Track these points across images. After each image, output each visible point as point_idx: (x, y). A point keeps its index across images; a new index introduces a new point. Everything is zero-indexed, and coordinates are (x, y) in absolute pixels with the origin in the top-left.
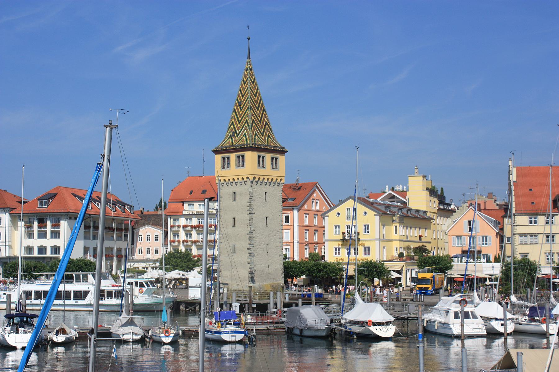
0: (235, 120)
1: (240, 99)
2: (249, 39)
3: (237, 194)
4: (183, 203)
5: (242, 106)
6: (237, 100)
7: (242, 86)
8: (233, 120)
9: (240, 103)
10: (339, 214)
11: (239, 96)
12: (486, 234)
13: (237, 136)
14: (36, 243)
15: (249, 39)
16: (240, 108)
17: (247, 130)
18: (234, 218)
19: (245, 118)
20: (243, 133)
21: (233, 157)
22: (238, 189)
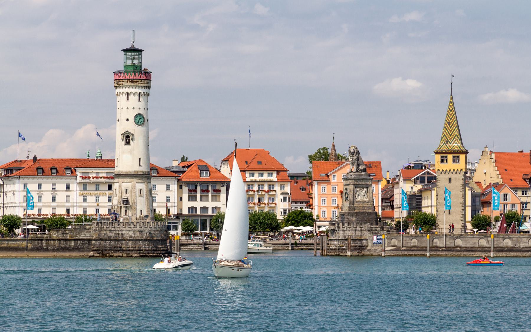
8: (445, 133)
9: (449, 123)
14: (198, 204)
22: (453, 176)
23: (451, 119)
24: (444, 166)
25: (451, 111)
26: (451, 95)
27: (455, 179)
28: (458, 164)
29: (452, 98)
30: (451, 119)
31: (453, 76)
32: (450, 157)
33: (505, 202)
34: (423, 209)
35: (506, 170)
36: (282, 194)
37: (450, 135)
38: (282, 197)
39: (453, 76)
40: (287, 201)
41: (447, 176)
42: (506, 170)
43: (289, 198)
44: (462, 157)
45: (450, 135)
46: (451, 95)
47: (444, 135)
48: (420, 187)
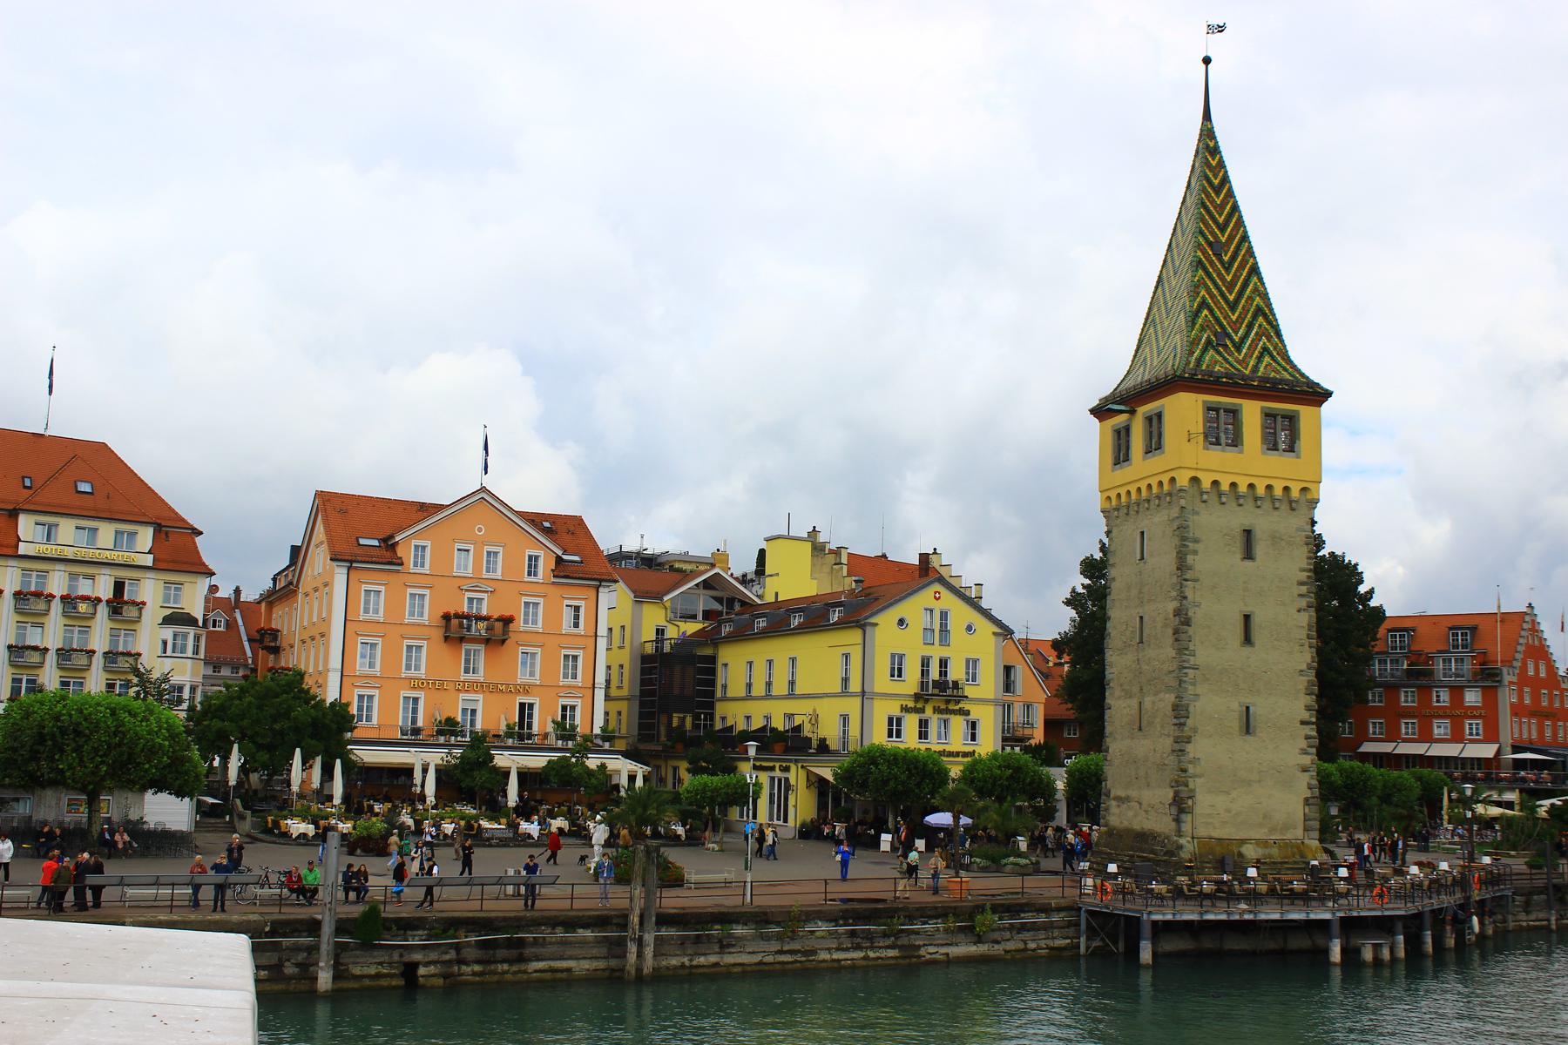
0: (1212, 296)
1: (1215, 236)
2: (1207, 61)
3: (1258, 534)
4: (13, 514)
5: (1226, 259)
6: (1201, 232)
7: (1208, 195)
9: (1217, 248)
10: (901, 622)
13: (1238, 348)
15: (1207, 61)
17: (1269, 338)
18: (1247, 618)
19: (1250, 299)
21: (1252, 412)
22: (1263, 523)
24: (1219, 465)
25: (1218, 193)
26: (1207, 115)
27: (1275, 539)
28: (1288, 459)
29: (1207, 133)
34: (721, 709)
36: (168, 621)
38: (168, 633)
40: (190, 653)
41: (1239, 518)
43: (197, 638)
45: (1233, 307)
46: (1207, 115)
47: (1203, 304)
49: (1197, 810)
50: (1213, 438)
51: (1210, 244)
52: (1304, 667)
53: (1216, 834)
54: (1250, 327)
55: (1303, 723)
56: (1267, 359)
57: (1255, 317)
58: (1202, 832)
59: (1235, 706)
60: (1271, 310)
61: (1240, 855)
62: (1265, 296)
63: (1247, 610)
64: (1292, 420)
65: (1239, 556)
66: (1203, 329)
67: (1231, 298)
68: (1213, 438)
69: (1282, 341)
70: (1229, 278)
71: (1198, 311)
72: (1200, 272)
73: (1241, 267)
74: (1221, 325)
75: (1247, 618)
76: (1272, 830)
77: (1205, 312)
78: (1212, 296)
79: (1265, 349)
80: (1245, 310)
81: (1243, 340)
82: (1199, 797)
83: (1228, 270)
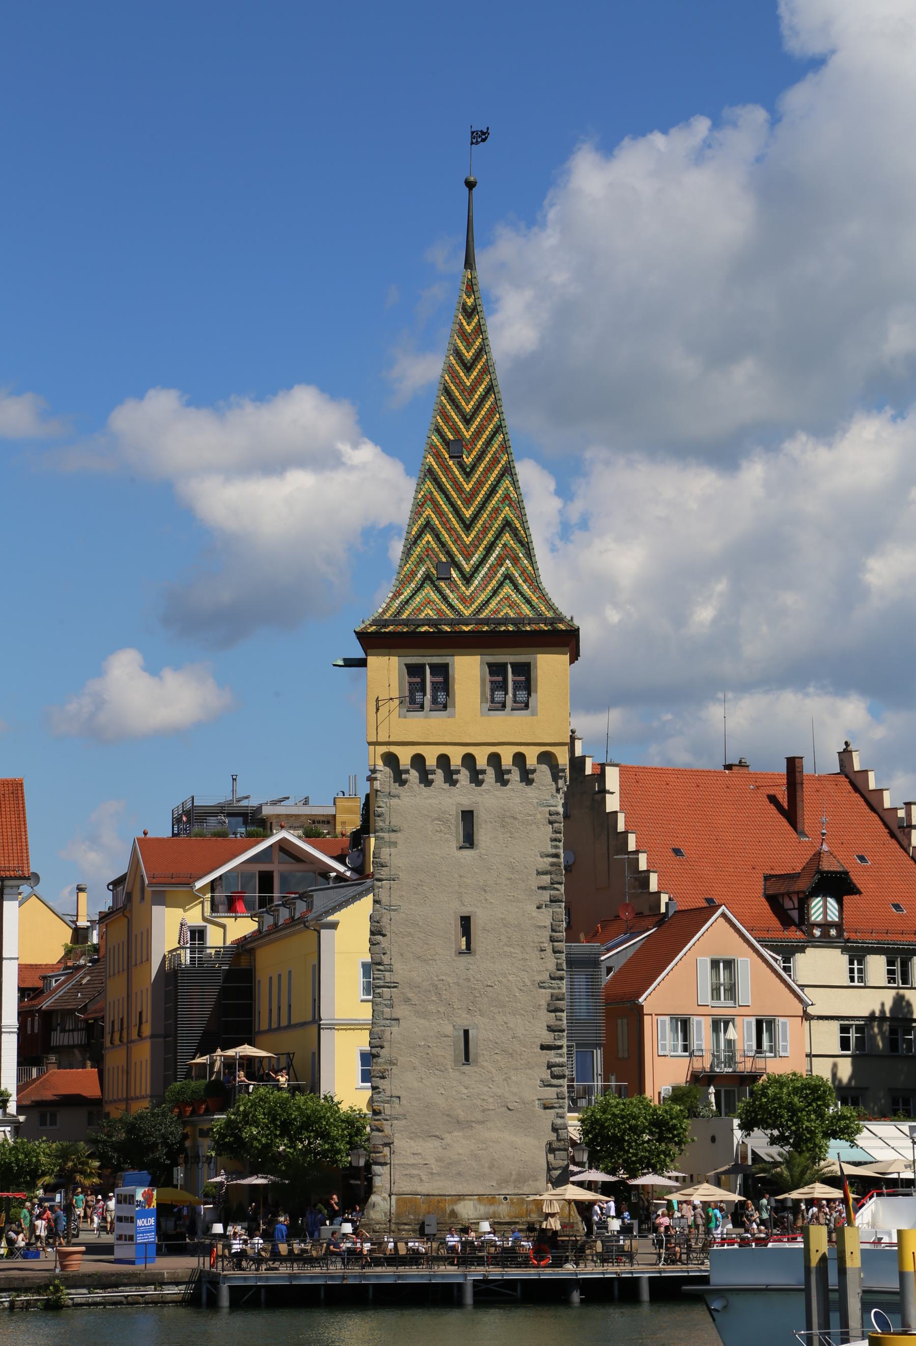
0: (440, 513)
1: (456, 431)
2: (470, 185)
3: (481, 818)
5: (468, 461)
6: (438, 431)
7: (454, 376)
8: (428, 511)
9: (455, 447)
11: (446, 418)
12: (681, 1011)
13: (467, 580)
15: (470, 185)
16: (461, 466)
17: (515, 560)
18: (466, 923)
19: (497, 510)
20: (493, 570)
22: (488, 799)
23: (468, 421)
25: (468, 368)
26: (469, 263)
27: (505, 820)
30: (468, 421)
31: (479, 137)
32: (468, 670)
33: (724, 1007)
35: (677, 852)
37: (468, 527)
39: (479, 137)
42: (677, 852)
44: (549, 666)
45: (468, 527)
48: (242, 926)
49: (395, 1160)
50: (412, 701)
51: (446, 442)
52: (546, 976)
53: (424, 1189)
54: (489, 549)
55: (543, 1047)
56: (507, 589)
57: (498, 536)
58: (404, 1186)
59: (449, 1029)
60: (523, 523)
61: (453, 1214)
62: (518, 507)
63: (465, 911)
64: (525, 671)
65: (454, 845)
66: (421, 561)
67: (468, 514)
68: (412, 701)
69: (532, 563)
70: (468, 487)
71: (419, 536)
72: (429, 484)
73: (488, 470)
74: (449, 553)
75: (466, 923)
76: (504, 1182)
77: (428, 537)
78: (440, 513)
79: (508, 577)
80: (485, 530)
81: (476, 569)
82: (399, 1143)
83: (468, 475)
